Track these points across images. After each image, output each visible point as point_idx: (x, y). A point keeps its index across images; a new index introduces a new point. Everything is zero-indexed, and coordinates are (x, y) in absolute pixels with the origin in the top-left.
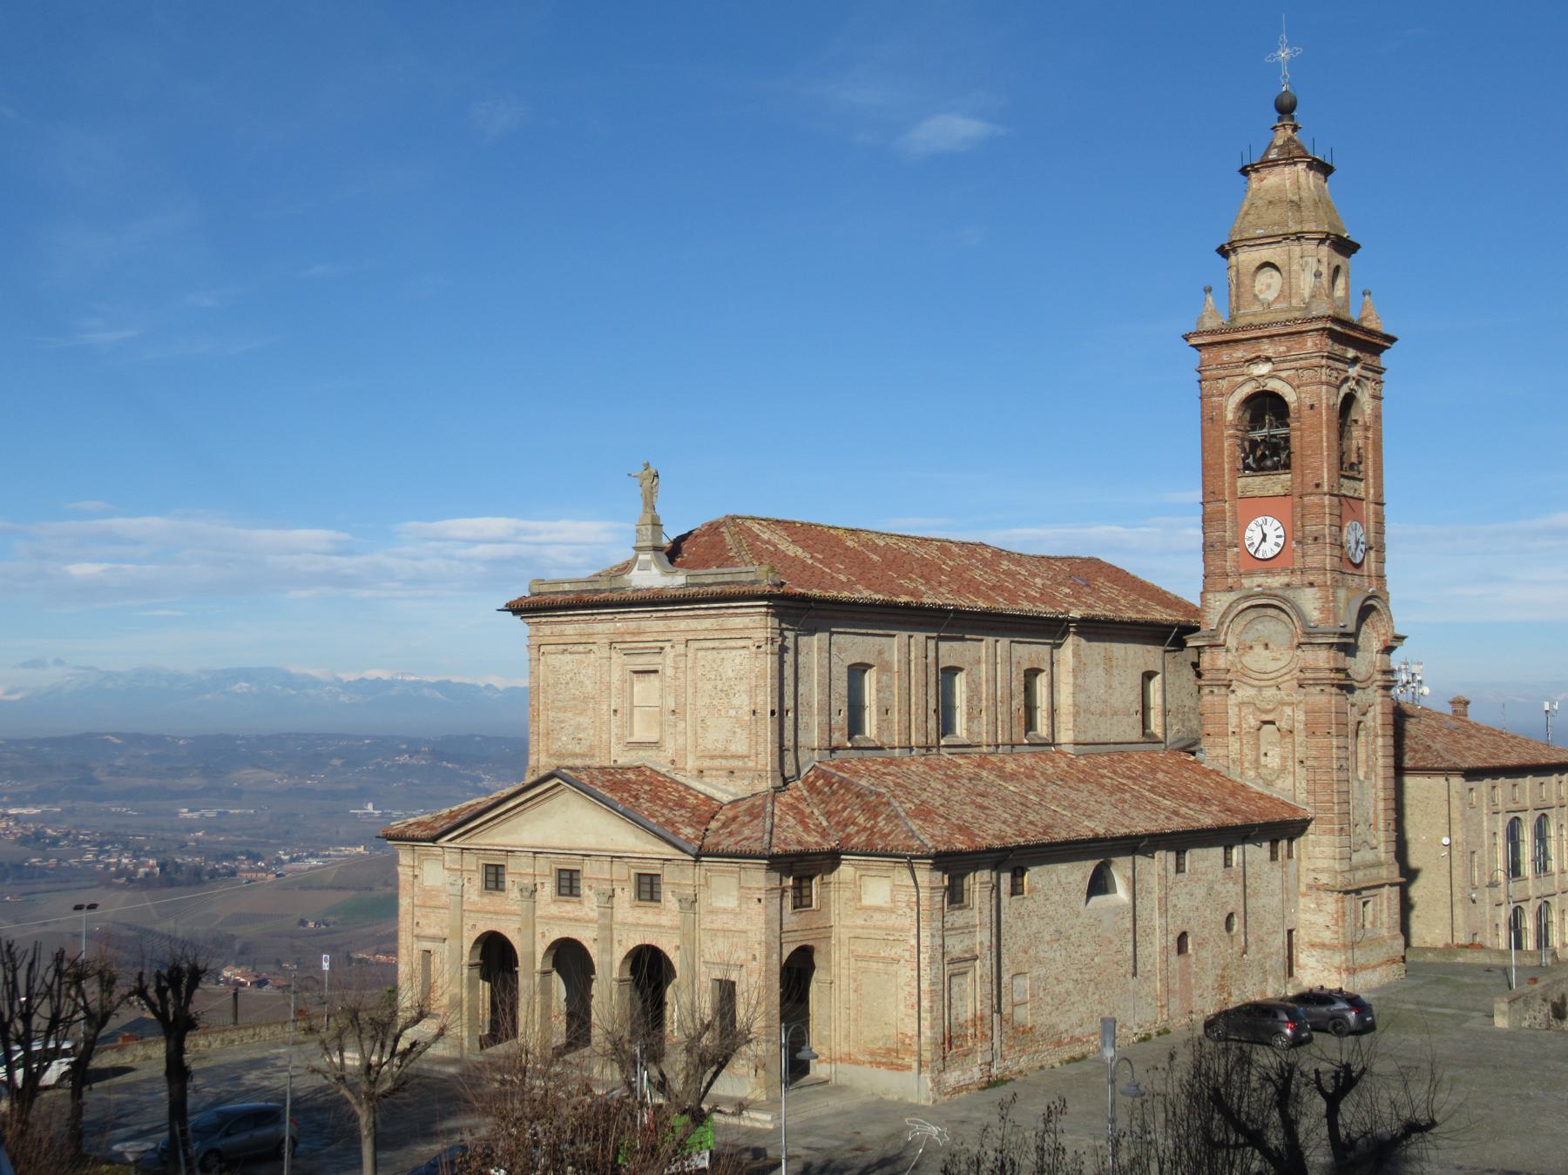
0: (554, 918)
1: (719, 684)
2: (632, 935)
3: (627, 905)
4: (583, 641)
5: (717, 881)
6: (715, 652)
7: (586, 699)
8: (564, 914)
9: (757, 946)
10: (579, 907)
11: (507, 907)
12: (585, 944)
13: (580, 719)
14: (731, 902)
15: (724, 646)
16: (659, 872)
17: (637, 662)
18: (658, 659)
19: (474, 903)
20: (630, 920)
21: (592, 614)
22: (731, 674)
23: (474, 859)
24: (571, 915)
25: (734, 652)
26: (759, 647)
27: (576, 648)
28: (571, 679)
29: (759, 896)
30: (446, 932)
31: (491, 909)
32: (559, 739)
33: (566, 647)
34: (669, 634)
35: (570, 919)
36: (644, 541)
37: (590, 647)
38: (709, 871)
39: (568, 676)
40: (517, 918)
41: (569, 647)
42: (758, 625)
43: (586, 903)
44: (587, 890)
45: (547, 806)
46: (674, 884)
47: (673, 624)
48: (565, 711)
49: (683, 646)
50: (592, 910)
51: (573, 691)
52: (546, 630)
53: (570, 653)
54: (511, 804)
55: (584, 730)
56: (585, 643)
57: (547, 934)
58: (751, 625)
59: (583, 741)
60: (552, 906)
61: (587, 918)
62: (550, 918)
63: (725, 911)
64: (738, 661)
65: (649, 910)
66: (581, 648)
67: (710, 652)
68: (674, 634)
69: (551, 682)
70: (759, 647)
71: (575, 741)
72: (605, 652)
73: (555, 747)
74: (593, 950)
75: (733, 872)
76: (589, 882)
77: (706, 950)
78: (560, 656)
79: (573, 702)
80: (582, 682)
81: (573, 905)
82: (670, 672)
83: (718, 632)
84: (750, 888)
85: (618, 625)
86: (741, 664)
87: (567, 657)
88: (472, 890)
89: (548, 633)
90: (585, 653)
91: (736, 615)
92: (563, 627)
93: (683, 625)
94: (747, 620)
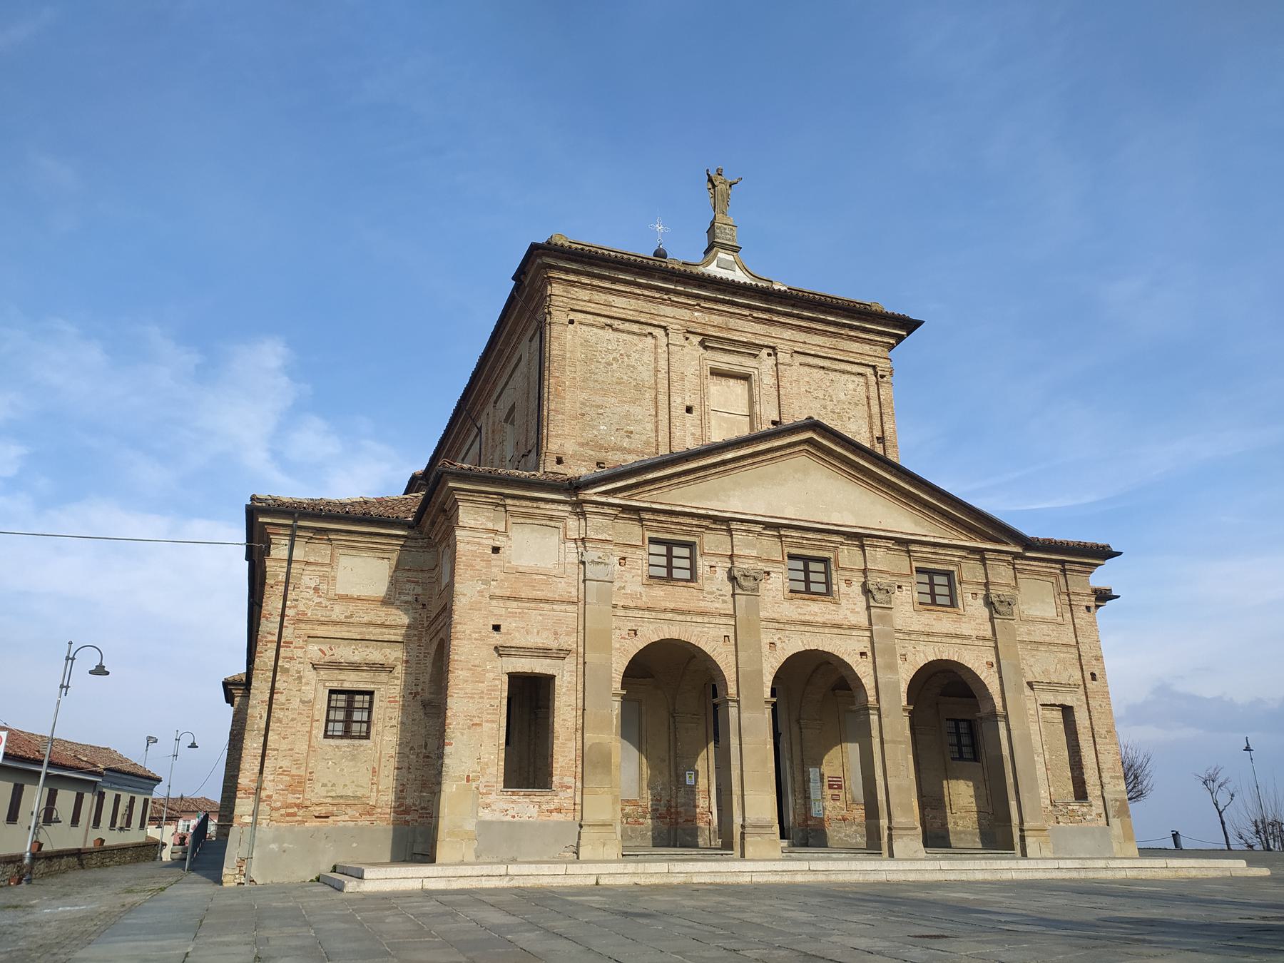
0: (793, 623)
1: (830, 406)
2: (921, 647)
3: (909, 608)
4: (643, 320)
5: (1025, 583)
6: (822, 372)
7: (638, 387)
8: (808, 618)
9: (1094, 662)
10: (833, 607)
11: (702, 604)
12: (847, 659)
13: (633, 409)
14: (1050, 613)
15: (837, 367)
16: (951, 568)
17: (722, 360)
18: (751, 362)
19: (632, 596)
20: (915, 627)
21: (668, 291)
22: (842, 397)
23: (636, 529)
24: (820, 619)
25: (846, 376)
26: (882, 377)
27: (627, 326)
28: (614, 359)
29: (1089, 604)
30: (569, 641)
31: (671, 605)
32: (593, 427)
33: (611, 322)
34: (769, 339)
35: (824, 625)
36: (729, 240)
37: (650, 329)
38: (1022, 571)
39: (611, 357)
40: (723, 621)
41: (616, 323)
42: (879, 355)
43: (843, 602)
44: (843, 584)
45: (769, 469)
46: (978, 584)
47: (774, 331)
48: (605, 395)
49: (789, 355)
50: (853, 611)
51: (617, 374)
52: (584, 294)
53: (615, 330)
54: (729, 455)
55: (638, 422)
56: (647, 327)
57: (778, 643)
58: (871, 353)
59: (634, 436)
60: (786, 604)
61: (846, 622)
62: (787, 623)
63: (1044, 621)
64: (851, 386)
65: (941, 615)
66: (635, 328)
67: (815, 370)
68: (775, 340)
69: (579, 355)
70: (882, 377)
71: (622, 433)
72: (677, 338)
73: (589, 434)
74: (863, 670)
75: (1050, 574)
76: (847, 575)
77: (1027, 669)
78: (595, 330)
79: (619, 387)
80: (633, 367)
81: (822, 605)
82: (769, 380)
83: (834, 351)
84: (1079, 594)
85: (696, 314)
86: (855, 391)
87: (609, 334)
88: (628, 576)
89: (587, 298)
90: (639, 334)
91: (856, 339)
92: (611, 298)
93: (788, 334)
94: (866, 348)
